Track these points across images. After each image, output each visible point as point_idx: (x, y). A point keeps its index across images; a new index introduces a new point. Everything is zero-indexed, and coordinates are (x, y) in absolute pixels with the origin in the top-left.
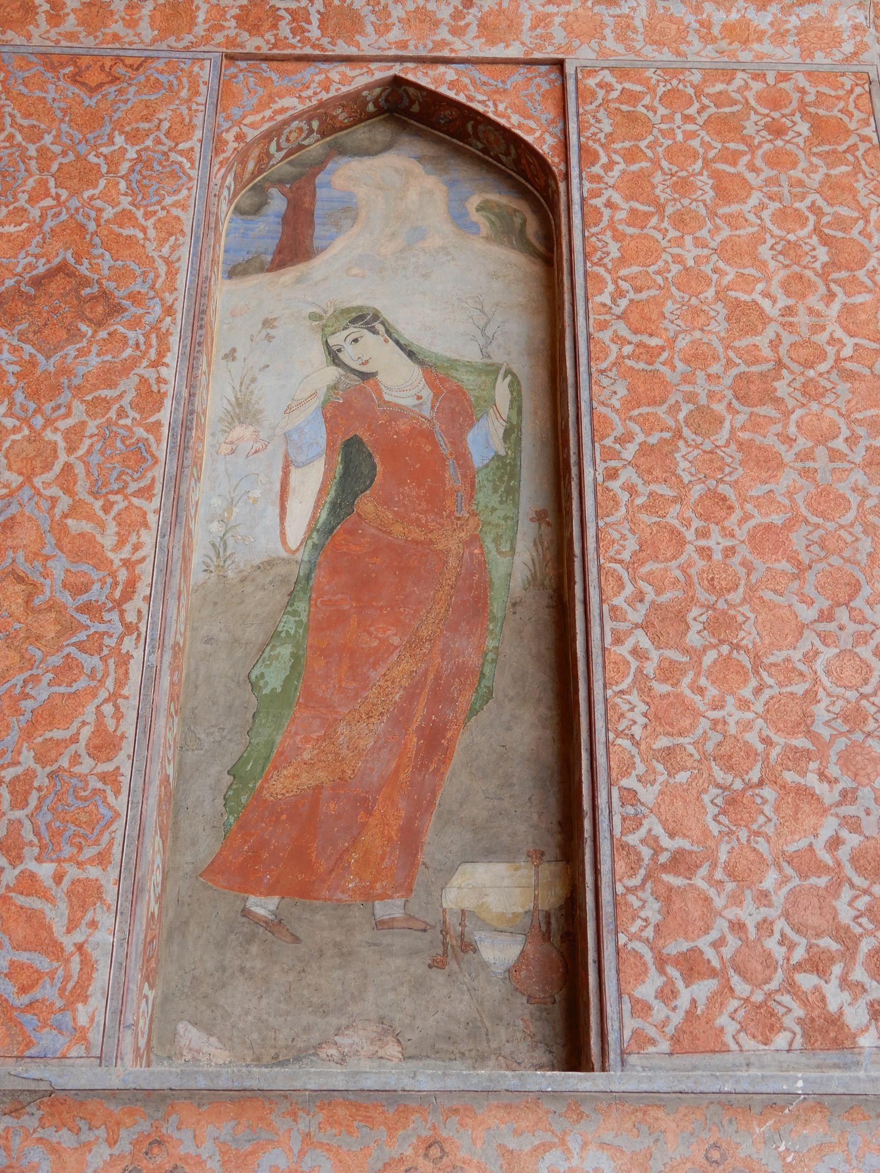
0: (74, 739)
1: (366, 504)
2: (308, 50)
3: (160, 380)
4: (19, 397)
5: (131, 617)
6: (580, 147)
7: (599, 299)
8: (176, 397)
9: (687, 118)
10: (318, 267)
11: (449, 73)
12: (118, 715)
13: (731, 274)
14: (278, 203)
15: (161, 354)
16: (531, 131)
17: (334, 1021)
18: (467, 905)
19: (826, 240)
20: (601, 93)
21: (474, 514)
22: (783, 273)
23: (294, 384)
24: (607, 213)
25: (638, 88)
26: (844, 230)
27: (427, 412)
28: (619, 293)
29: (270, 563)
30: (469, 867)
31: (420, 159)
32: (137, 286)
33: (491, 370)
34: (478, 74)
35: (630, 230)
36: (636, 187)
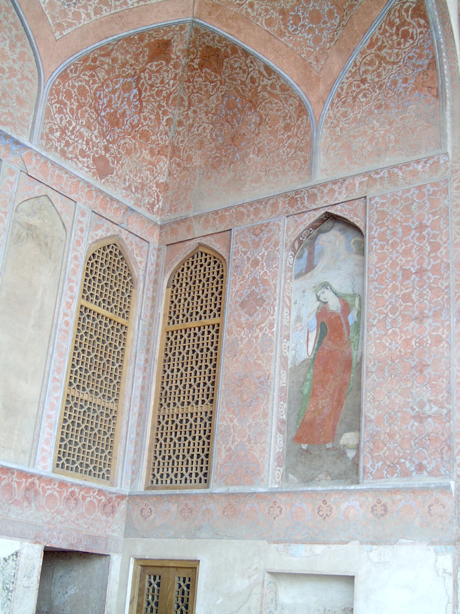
0: (259, 415)
1: (326, 339)
2: (305, 210)
3: (274, 319)
4: (245, 329)
5: (269, 384)
6: (369, 226)
7: (371, 276)
8: (278, 324)
9: (398, 209)
10: (315, 272)
11: (339, 207)
12: (267, 408)
13: (404, 260)
14: (306, 254)
15: (274, 312)
16: (358, 222)
17: (318, 472)
18: (345, 443)
19: (430, 244)
20: (375, 205)
21: (349, 340)
22: (418, 258)
23: (309, 309)
24: (374, 246)
25: (385, 201)
26: (435, 239)
27: (339, 311)
28: (376, 273)
29: (305, 361)
30: (345, 434)
31: (340, 230)
32: (269, 294)
33: (354, 296)
34: (346, 206)
35: (380, 251)
36: (382, 237)
